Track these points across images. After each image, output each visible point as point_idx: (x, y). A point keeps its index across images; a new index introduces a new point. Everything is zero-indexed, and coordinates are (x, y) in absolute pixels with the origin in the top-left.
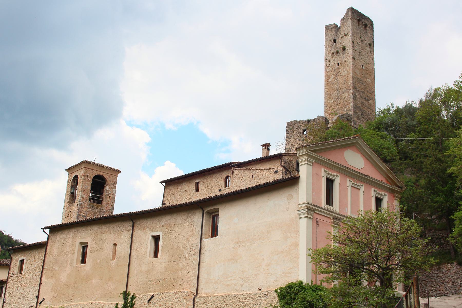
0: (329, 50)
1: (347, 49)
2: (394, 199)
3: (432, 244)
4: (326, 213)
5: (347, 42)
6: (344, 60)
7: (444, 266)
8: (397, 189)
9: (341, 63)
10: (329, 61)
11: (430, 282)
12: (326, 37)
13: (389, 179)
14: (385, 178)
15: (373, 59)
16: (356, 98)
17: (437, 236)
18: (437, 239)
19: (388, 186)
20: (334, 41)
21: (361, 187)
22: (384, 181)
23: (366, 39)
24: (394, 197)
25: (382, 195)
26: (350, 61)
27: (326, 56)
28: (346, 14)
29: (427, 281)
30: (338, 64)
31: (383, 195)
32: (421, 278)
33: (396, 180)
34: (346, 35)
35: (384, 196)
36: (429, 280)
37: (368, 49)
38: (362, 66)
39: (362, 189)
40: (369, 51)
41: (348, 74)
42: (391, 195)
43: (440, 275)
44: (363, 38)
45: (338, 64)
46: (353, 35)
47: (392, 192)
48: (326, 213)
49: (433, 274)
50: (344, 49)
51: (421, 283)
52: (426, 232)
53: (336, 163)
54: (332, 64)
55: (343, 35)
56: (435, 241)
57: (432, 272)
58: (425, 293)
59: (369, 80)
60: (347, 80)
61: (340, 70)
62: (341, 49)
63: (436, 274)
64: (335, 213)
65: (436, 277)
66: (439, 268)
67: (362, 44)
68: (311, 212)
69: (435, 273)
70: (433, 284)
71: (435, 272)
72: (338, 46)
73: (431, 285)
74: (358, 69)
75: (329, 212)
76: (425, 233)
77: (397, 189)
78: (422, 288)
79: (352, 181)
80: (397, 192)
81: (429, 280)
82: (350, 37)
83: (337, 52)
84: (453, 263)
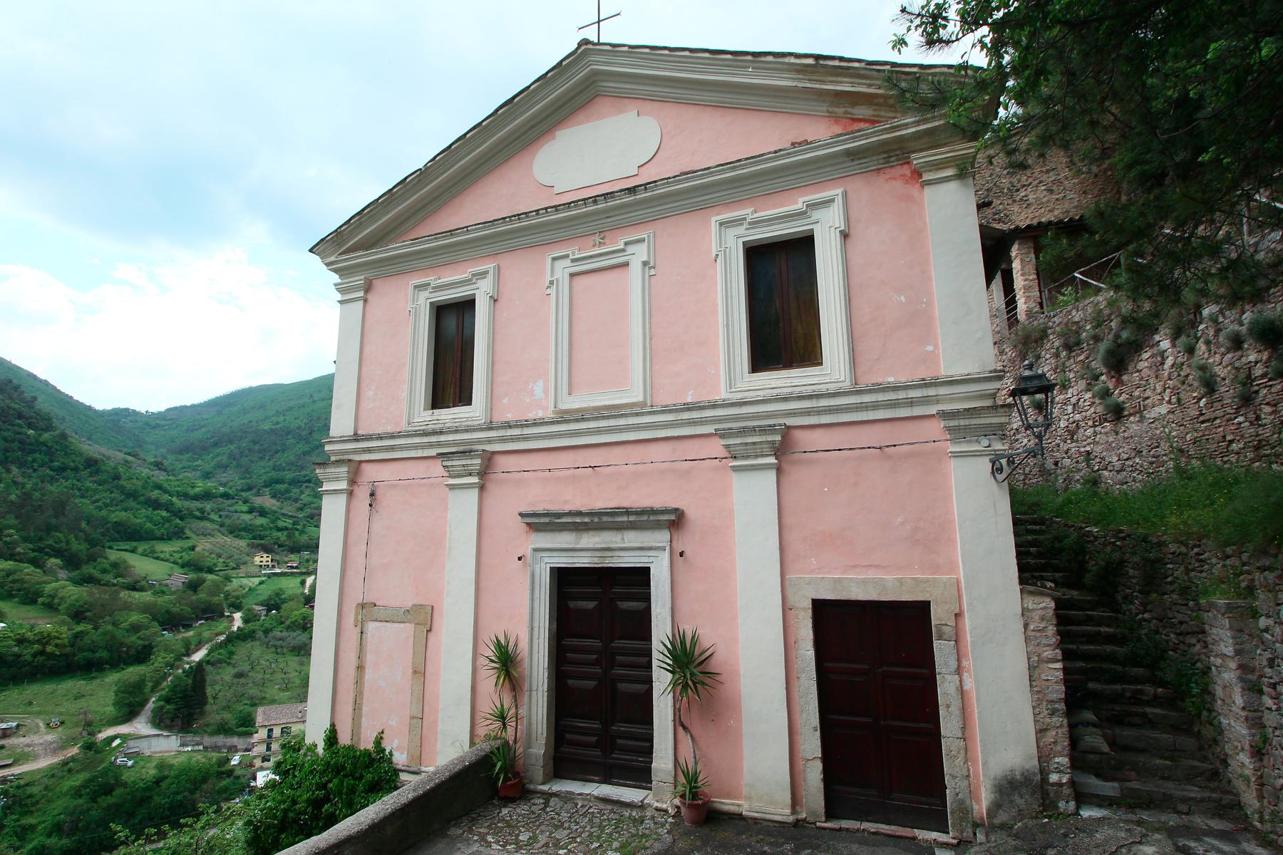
2: (914, 190)
13: (853, 105)
21: (630, 249)
24: (917, 174)
25: (801, 215)
35: (816, 215)
42: (887, 180)
53: (451, 232)
64: (456, 431)
68: (333, 470)
75: (426, 439)
79: (567, 256)
80: (930, 139)
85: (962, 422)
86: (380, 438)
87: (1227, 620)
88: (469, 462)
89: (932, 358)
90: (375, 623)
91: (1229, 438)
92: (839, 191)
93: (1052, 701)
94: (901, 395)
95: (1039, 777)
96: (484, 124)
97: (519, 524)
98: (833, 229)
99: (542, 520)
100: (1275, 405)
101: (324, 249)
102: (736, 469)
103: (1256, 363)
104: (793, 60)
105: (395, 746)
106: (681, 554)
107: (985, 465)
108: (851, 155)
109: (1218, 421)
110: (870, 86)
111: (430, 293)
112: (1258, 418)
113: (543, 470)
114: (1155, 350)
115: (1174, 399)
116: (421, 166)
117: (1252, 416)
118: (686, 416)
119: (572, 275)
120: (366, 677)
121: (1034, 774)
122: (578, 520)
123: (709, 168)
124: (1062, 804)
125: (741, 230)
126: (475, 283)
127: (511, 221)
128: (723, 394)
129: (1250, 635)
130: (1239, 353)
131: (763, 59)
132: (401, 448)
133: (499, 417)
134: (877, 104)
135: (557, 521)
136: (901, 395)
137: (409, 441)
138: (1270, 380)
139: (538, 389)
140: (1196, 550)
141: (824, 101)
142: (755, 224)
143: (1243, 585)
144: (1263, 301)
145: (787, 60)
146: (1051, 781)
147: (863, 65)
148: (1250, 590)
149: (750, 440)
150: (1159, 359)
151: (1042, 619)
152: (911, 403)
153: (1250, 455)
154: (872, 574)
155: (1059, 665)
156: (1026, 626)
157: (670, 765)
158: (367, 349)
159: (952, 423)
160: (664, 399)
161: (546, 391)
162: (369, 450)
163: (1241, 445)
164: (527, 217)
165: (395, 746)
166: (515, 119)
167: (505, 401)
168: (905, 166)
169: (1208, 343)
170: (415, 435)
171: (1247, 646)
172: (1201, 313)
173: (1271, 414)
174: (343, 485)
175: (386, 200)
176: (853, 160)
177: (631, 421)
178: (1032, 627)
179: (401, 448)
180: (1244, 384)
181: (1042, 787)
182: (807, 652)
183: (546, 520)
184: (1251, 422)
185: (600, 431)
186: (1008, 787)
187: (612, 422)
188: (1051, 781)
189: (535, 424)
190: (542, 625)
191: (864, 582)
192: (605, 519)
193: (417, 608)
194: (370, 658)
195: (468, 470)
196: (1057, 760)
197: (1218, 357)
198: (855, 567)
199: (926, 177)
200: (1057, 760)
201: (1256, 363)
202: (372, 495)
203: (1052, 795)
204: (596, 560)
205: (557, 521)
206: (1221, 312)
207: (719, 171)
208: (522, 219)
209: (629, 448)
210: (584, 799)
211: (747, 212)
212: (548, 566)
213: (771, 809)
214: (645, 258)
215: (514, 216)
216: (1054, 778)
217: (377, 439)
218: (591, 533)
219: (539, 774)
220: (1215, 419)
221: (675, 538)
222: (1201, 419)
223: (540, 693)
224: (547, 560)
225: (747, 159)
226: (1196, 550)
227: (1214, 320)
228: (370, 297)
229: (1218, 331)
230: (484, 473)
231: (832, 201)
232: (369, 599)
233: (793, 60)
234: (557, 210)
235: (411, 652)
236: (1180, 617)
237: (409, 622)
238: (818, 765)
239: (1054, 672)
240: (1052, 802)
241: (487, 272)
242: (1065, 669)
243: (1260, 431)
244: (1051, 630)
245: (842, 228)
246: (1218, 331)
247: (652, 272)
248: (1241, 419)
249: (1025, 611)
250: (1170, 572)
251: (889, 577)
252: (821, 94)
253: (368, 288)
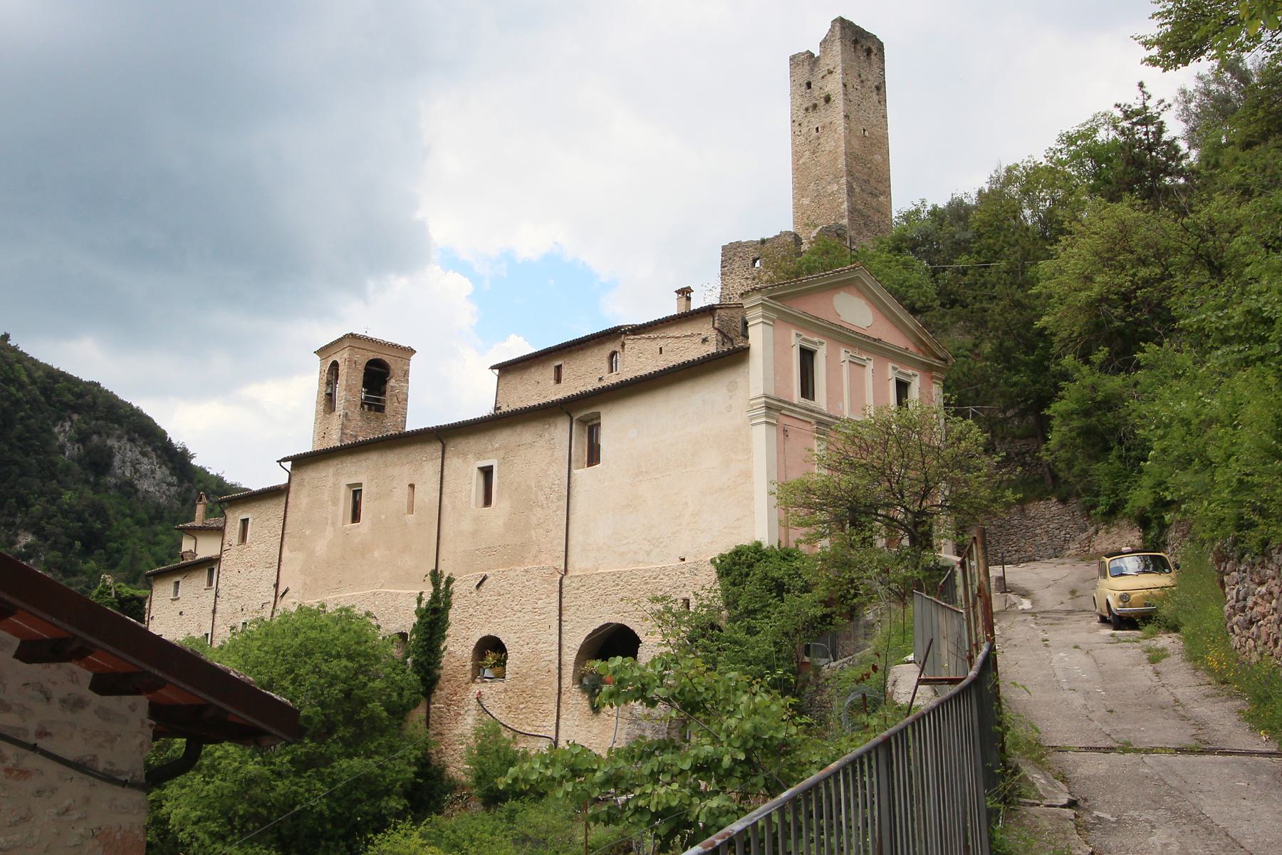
0: (798, 103)
1: (833, 99)
2: (931, 382)
5: (834, 85)
6: (828, 120)
7: (1031, 505)
9: (824, 127)
10: (800, 125)
12: (793, 79)
14: (914, 344)
15: (885, 117)
16: (852, 192)
18: (1017, 455)
19: (921, 358)
20: (809, 85)
21: (867, 361)
22: (912, 348)
23: (870, 77)
24: (932, 378)
25: (908, 376)
26: (840, 123)
27: (792, 114)
28: (830, 30)
30: (817, 129)
34: (830, 72)
35: (913, 378)
36: (1004, 533)
37: (875, 98)
38: (864, 130)
39: (870, 366)
40: (877, 102)
41: (837, 147)
43: (1026, 522)
44: (863, 77)
45: (817, 129)
46: (845, 72)
47: (928, 368)
50: (828, 99)
52: (996, 443)
54: (804, 130)
55: (826, 72)
59: (878, 157)
60: (836, 159)
61: (822, 140)
62: (823, 100)
64: (819, 413)
66: (1023, 510)
67: (863, 87)
72: (816, 94)
74: (856, 136)
76: (994, 445)
77: (937, 363)
80: (938, 369)
81: (1004, 533)
82: (838, 76)
83: (815, 106)
84: (1050, 499)
137: (801, 410)
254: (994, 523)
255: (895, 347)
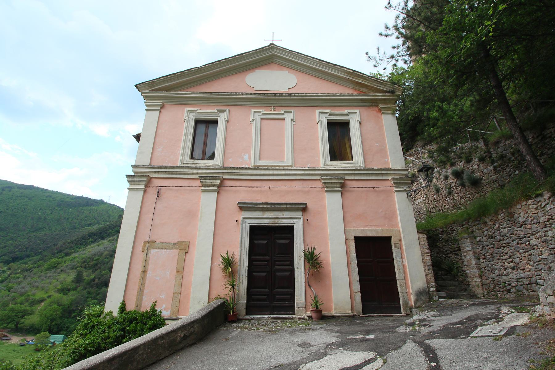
2: (379, 115)
3: (505, 166)
4: (185, 173)
7: (519, 206)
8: (382, 96)
11: (498, 248)
13: (362, 87)
14: (354, 89)
17: (512, 148)
18: (513, 154)
21: (286, 114)
24: (380, 110)
25: (346, 115)
29: (493, 248)
31: (348, 114)
32: (480, 241)
33: (375, 84)
35: (351, 116)
43: (517, 230)
48: (185, 173)
49: (501, 230)
51: (482, 252)
52: (492, 150)
53: (211, 93)
56: (510, 158)
57: (497, 225)
58: (493, 276)
63: (506, 229)
64: (208, 168)
65: (508, 235)
66: (511, 215)
68: (137, 179)
69: (505, 228)
70: (506, 253)
71: (505, 225)
73: (502, 256)
77: (380, 96)
78: (486, 263)
79: (260, 112)
80: (385, 101)
81: (496, 246)
84: (541, 195)
85: (399, 181)
86: (166, 167)
87: (469, 240)
88: (214, 181)
89: (387, 162)
90: (155, 250)
91: (444, 205)
92: (358, 110)
93: (429, 266)
94: (380, 172)
95: (427, 290)
96: (229, 59)
97: (236, 207)
98: (357, 121)
99: (249, 206)
100: (459, 194)
101: (143, 87)
102: (327, 191)
103: (452, 183)
104: (346, 69)
105: (163, 308)
106: (307, 220)
107: (405, 195)
108: (362, 100)
109: (441, 200)
110: (368, 83)
111: (196, 114)
112: (453, 198)
113: (249, 187)
114: (418, 183)
115: (425, 196)
116: (199, 66)
117: (451, 197)
118: (308, 172)
119: (262, 119)
120: (148, 276)
121: (426, 289)
122: (265, 206)
123: (318, 94)
124: (434, 298)
125: (326, 116)
126: (218, 114)
127: (239, 94)
128: (322, 166)
129: (474, 244)
130: (447, 180)
131: (336, 67)
132: (176, 173)
133: (226, 165)
134: (369, 89)
135: (255, 206)
136: (380, 172)
137: (182, 170)
138: (457, 187)
139: (246, 157)
140: (450, 228)
141: (352, 84)
142: (331, 115)
143: (470, 231)
144: (454, 166)
145: (344, 69)
146: (431, 290)
147: (367, 76)
148: (473, 232)
149: (333, 181)
150: (420, 185)
151: (424, 241)
152: (383, 175)
153: (451, 209)
154: (373, 228)
155: (429, 254)
156: (420, 243)
157: (304, 300)
158: (159, 131)
159: (396, 181)
160: (299, 166)
161: (249, 158)
162: (158, 173)
163: (448, 206)
164: (246, 94)
165: (163, 308)
166: (241, 61)
167: (231, 160)
168: (377, 108)
169: (437, 179)
170: (185, 168)
171: (474, 247)
172: (434, 171)
173: (457, 196)
174: (143, 186)
175: (180, 74)
176: (362, 102)
177: (287, 172)
178: (421, 243)
179: (176, 173)
180: (449, 189)
181: (428, 293)
182: (354, 255)
183: (251, 206)
184: (451, 200)
185: (274, 175)
186: (419, 294)
187: (279, 172)
188: (431, 290)
189: (246, 169)
190: (246, 248)
191: (371, 230)
192: (277, 206)
193: (180, 243)
194: (150, 267)
195: (213, 184)
196: (432, 284)
197: (440, 182)
198: (368, 225)
199: (383, 112)
200: (432, 284)
201: (452, 183)
202: (158, 192)
203: (431, 295)
204: (271, 222)
205: (255, 206)
206: (441, 169)
207: (321, 95)
208: (244, 95)
209: (285, 182)
210: (265, 320)
211: (329, 111)
212: (249, 225)
213: (344, 312)
214: (292, 118)
215: (241, 93)
216: (431, 289)
217: (164, 168)
218: (269, 212)
219: (244, 311)
220: (440, 200)
221: (304, 215)
222: (435, 201)
223: (244, 277)
224: (248, 222)
225: (331, 94)
226: (450, 228)
227: (438, 172)
228: (162, 111)
229: (440, 175)
230: (220, 186)
231: (356, 112)
232: (152, 239)
233: (346, 69)
234: (259, 95)
235: (176, 262)
236: (446, 249)
237: (176, 249)
238: (359, 294)
239: (428, 257)
240: (432, 297)
241: (225, 111)
242: (431, 256)
243: (454, 201)
244: (426, 244)
245: (360, 121)
246: (440, 175)
247: (294, 123)
248: (448, 199)
249: (419, 238)
250: (441, 237)
251: (379, 229)
252: (352, 82)
253: (162, 107)
254: (485, 233)
255: (317, 95)
